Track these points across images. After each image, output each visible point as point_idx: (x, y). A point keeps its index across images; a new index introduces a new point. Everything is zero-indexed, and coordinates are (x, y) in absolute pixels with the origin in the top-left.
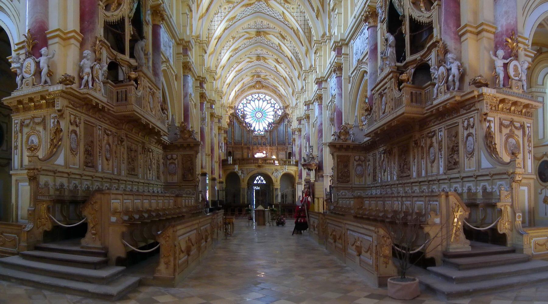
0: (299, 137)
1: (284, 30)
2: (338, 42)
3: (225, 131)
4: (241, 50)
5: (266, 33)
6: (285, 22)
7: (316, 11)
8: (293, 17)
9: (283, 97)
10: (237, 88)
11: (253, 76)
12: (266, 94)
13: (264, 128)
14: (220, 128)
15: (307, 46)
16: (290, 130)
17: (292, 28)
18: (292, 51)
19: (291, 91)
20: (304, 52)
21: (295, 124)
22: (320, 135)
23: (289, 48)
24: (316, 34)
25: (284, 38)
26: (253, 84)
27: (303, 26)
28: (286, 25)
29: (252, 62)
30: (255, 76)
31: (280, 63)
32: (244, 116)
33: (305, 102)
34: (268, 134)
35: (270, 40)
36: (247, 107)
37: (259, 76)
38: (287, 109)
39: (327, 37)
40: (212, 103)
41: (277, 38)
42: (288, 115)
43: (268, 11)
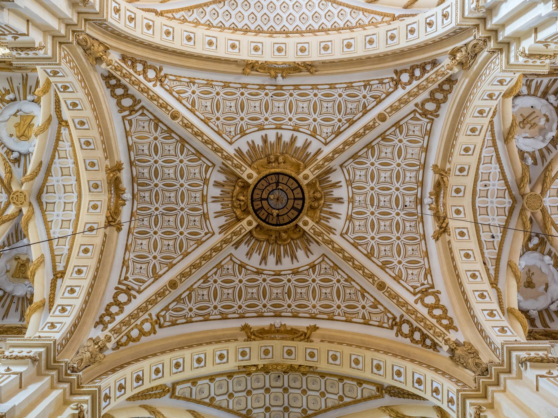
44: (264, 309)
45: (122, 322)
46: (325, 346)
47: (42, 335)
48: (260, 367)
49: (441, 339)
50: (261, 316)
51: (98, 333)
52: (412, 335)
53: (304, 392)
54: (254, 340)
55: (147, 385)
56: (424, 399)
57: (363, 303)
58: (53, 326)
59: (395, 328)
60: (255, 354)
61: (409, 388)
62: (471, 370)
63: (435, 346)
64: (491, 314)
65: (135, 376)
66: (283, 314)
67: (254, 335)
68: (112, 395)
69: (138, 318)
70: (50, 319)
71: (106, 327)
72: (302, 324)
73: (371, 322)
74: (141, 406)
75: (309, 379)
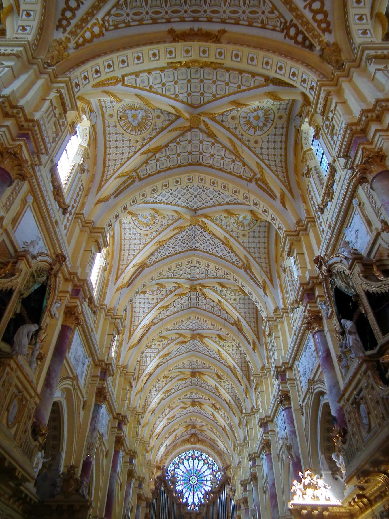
0: (246, 512)
1: (221, 369)
2: (281, 367)
3: (147, 504)
4: (174, 392)
5: (201, 373)
6: (221, 360)
7: (252, 344)
8: (229, 354)
9: (222, 454)
10: (167, 442)
11: (187, 427)
12: (202, 451)
13: (200, 499)
14: (140, 497)
15: (246, 385)
16: (233, 503)
17: (229, 367)
18: (230, 393)
19: (231, 443)
20: (243, 392)
21: (239, 494)
22: (273, 503)
23: (227, 390)
24: (255, 366)
25: (220, 378)
26: (187, 437)
27: (240, 364)
28: (222, 363)
29: (186, 408)
30: (190, 427)
31: (217, 409)
32: (174, 481)
33: (249, 455)
34: (205, 509)
35: (206, 382)
36: (179, 468)
37: (194, 427)
38: (228, 471)
39: (267, 368)
40: (132, 455)
41: (214, 379)
42: (230, 478)
43: (203, 350)
44: (186, 15)
45: (77, 26)
46: (230, 47)
47: (18, 36)
48: (183, 64)
49: (316, 40)
50: (182, 20)
51: (59, 35)
52: (296, 37)
53: (214, 82)
54: (178, 42)
55: (104, 77)
56: (295, 87)
57: (264, 9)
58: (24, 29)
59: (285, 31)
60: (179, 53)
61: (286, 79)
62: (332, 65)
63: (311, 47)
64: (361, 19)
65: (94, 69)
66: (200, 19)
67: (178, 37)
68: (80, 84)
69: (88, 22)
70: (21, 23)
71: (65, 31)
72: (214, 28)
73: (267, 27)
74: (102, 91)
75: (218, 73)
